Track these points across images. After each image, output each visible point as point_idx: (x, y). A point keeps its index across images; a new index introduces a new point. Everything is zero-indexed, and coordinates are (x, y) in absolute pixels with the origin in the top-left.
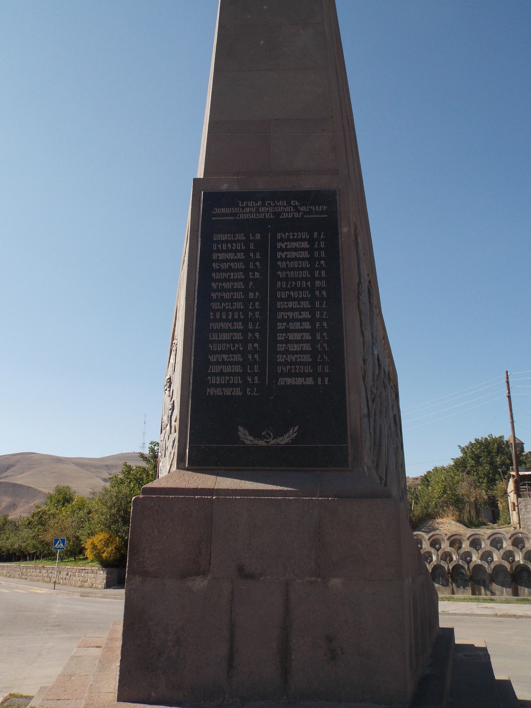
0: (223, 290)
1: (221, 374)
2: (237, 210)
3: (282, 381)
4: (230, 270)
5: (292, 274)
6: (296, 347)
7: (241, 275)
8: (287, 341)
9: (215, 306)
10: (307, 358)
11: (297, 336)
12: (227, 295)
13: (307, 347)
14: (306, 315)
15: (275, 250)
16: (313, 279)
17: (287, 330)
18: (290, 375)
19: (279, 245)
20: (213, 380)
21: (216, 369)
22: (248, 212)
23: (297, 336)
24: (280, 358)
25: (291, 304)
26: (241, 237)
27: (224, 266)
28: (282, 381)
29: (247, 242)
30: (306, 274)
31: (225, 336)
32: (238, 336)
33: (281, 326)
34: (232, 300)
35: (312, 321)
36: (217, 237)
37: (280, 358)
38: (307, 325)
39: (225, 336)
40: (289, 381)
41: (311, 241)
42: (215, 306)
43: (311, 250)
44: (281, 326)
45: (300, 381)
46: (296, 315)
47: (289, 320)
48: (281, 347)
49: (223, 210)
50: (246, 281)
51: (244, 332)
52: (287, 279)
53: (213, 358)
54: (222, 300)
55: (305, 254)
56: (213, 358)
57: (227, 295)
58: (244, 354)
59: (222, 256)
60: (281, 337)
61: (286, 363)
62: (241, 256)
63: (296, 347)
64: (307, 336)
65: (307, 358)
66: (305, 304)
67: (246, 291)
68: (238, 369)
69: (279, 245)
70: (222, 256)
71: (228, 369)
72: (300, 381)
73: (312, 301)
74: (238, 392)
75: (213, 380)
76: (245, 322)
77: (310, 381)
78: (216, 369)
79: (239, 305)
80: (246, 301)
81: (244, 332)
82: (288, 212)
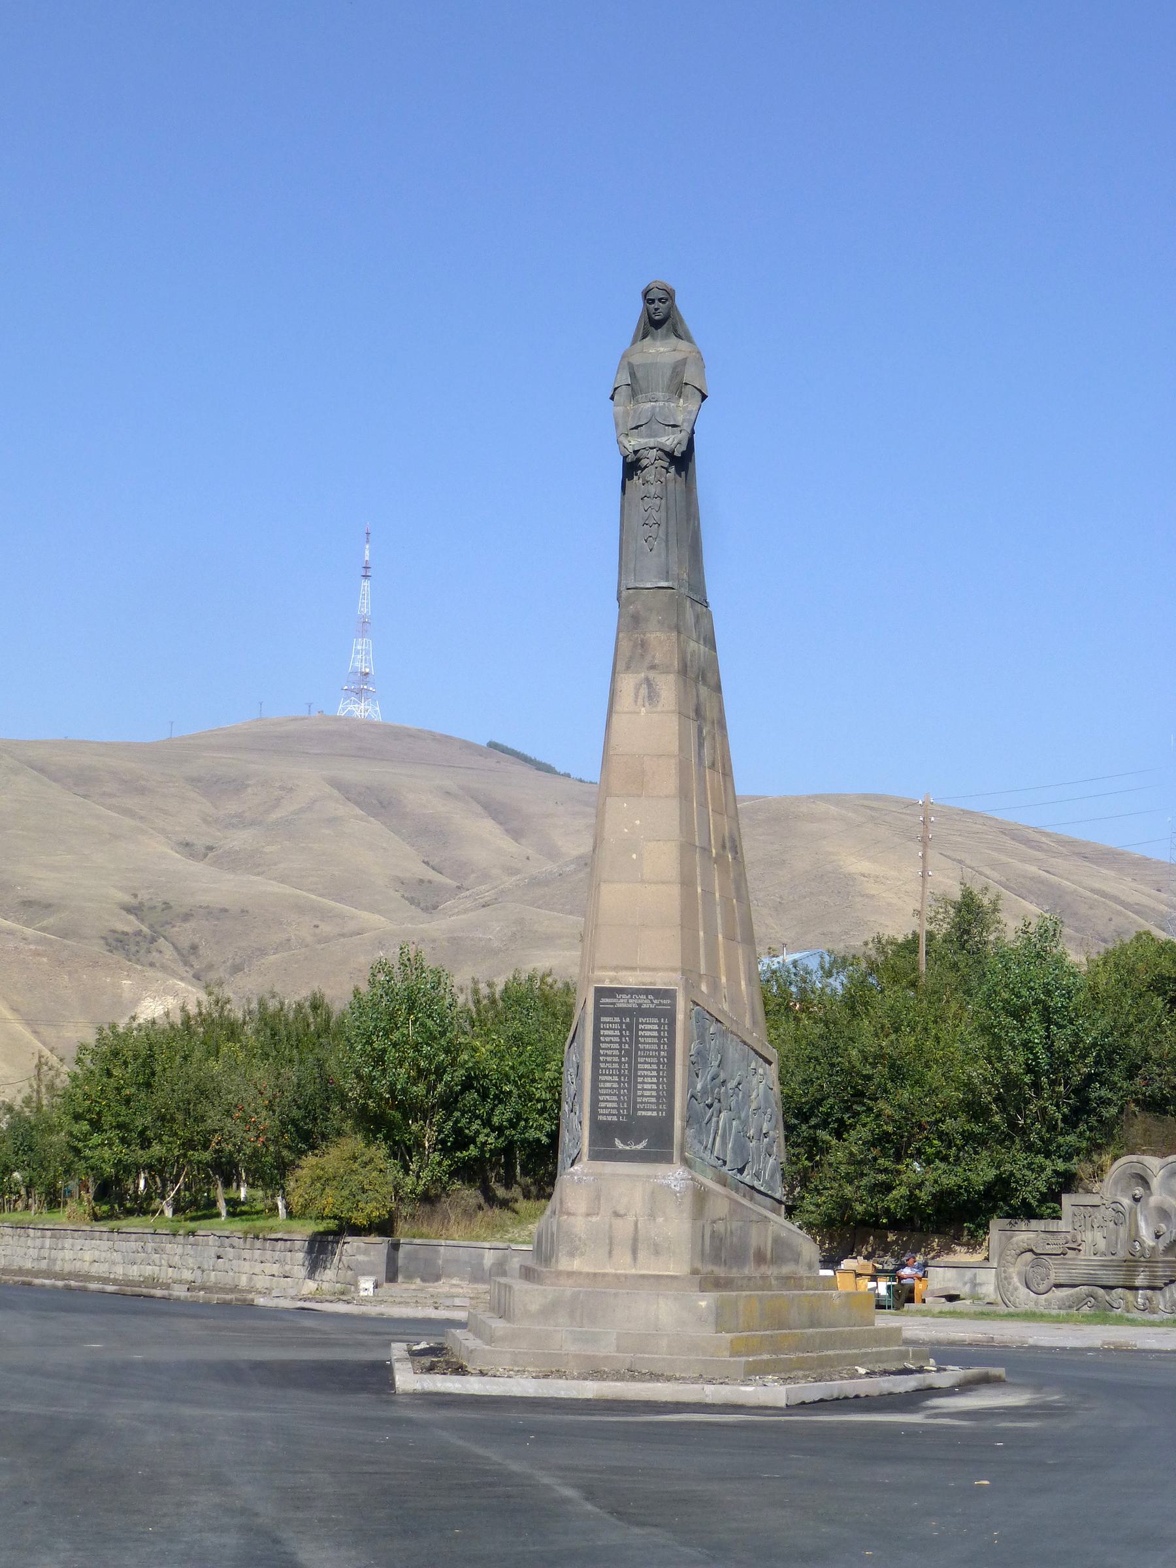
0: (606, 1055)
1: (606, 1108)
2: (614, 1001)
3: (639, 1113)
4: (611, 1042)
5: (647, 1047)
6: (647, 1093)
7: (617, 1046)
8: (643, 1089)
9: (602, 1065)
10: (654, 1100)
11: (649, 1086)
12: (609, 1059)
13: (654, 1093)
14: (654, 1073)
15: (638, 1030)
16: (659, 1050)
17: (643, 1083)
18: (644, 1110)
19: (641, 1026)
20: (601, 1111)
21: (602, 1105)
22: (622, 1002)
23: (649, 1086)
24: (639, 1100)
25: (646, 1066)
26: (617, 1019)
27: (608, 1039)
28: (639, 1113)
29: (621, 1023)
30: (655, 1047)
31: (608, 1085)
32: (615, 1085)
33: (640, 1080)
34: (612, 1062)
35: (658, 1077)
36: (603, 1019)
37: (639, 1100)
38: (655, 1080)
39: (608, 1085)
40: (644, 1113)
41: (659, 1025)
42: (602, 1065)
43: (659, 1031)
44: (640, 1080)
45: (649, 1113)
46: (649, 1073)
47: (644, 1076)
48: (639, 1093)
49: (607, 1000)
50: (620, 1050)
51: (619, 1082)
52: (644, 1050)
53: (601, 1098)
54: (606, 1062)
55: (655, 1034)
56: (601, 1098)
57: (609, 1059)
58: (619, 1096)
59: (606, 1032)
60: (639, 1087)
61: (642, 1103)
62: (617, 1033)
63: (647, 1093)
64: (655, 1087)
65: (654, 1100)
66: (655, 1067)
67: (620, 1057)
68: (615, 1105)
69: (641, 1026)
70: (606, 1032)
71: (610, 1105)
72: (649, 1113)
73: (658, 1064)
74: (615, 1118)
75: (601, 1111)
76: (619, 1076)
77: (655, 1114)
78: (602, 1105)
79: (616, 1066)
80: (620, 1063)
81: (619, 1082)
82: (646, 1003)
